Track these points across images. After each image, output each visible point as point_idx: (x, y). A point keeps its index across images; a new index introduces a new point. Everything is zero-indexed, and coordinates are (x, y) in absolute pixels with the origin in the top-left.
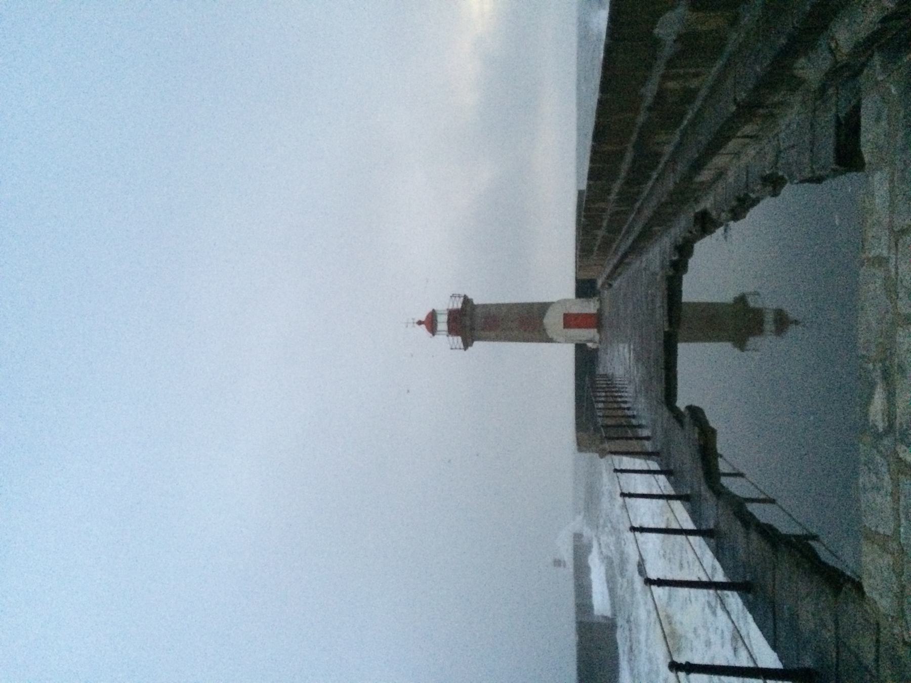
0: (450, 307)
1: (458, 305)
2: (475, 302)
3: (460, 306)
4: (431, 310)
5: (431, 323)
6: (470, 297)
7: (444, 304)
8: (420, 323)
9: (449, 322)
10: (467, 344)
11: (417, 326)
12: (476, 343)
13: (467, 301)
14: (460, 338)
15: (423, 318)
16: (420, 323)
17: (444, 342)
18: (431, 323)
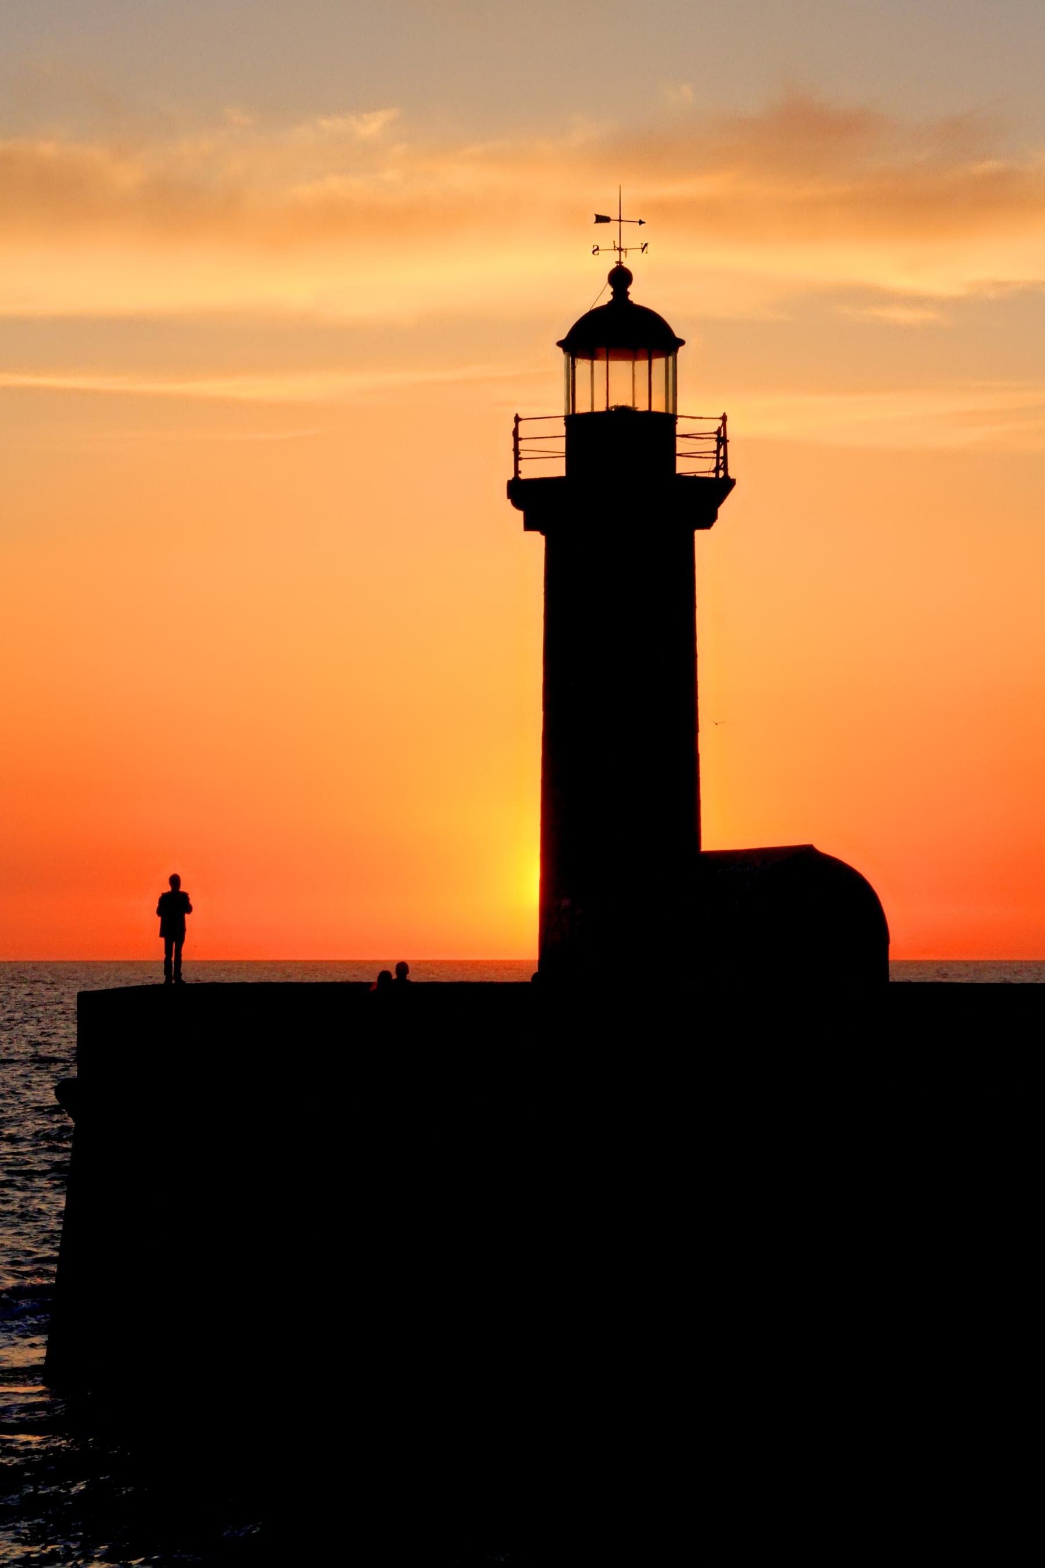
2: (699, 535)
3: (683, 466)
5: (621, 328)
8: (620, 278)
14: (549, 463)
15: (637, 295)
16: (620, 278)
17: (537, 403)
18: (621, 328)
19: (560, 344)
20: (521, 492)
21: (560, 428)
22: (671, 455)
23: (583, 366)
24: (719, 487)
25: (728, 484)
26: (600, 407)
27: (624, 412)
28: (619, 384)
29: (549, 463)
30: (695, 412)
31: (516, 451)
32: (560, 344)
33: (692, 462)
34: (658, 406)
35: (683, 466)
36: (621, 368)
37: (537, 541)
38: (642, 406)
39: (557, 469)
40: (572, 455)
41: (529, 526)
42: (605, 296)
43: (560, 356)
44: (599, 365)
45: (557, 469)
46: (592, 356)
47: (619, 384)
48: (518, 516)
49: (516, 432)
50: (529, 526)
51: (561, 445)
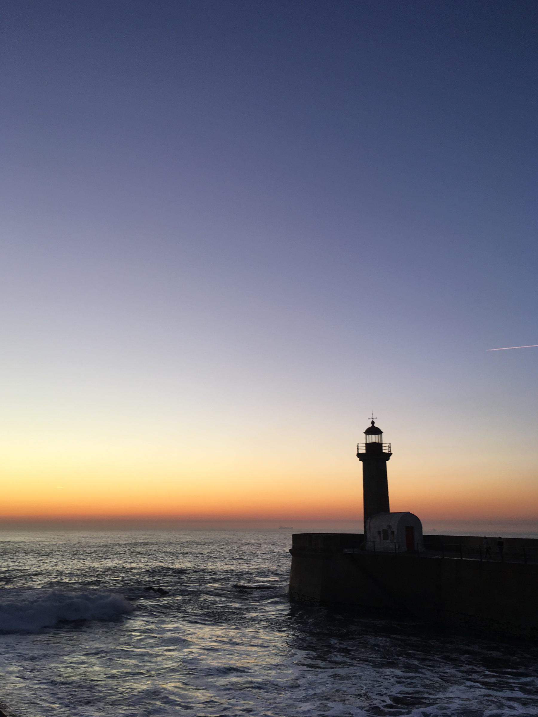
0: (383, 445)
1: (385, 450)
2: (387, 462)
3: (384, 451)
5: (373, 430)
6: (391, 457)
7: (387, 440)
8: (373, 423)
9: (374, 444)
10: (359, 455)
11: (371, 420)
13: (388, 456)
14: (363, 451)
15: (376, 425)
16: (373, 423)
18: (373, 430)
19: (364, 433)
21: (364, 445)
23: (368, 436)
24: (390, 454)
25: (391, 454)
26: (371, 442)
28: (373, 439)
31: (358, 449)
32: (364, 433)
35: (384, 451)
36: (373, 436)
37: (361, 463)
38: (377, 442)
39: (364, 451)
40: (367, 449)
41: (360, 460)
42: (371, 425)
43: (364, 435)
44: (370, 436)
46: (369, 434)
47: (373, 439)
48: (358, 459)
49: (358, 446)
50: (360, 460)
51: (365, 448)
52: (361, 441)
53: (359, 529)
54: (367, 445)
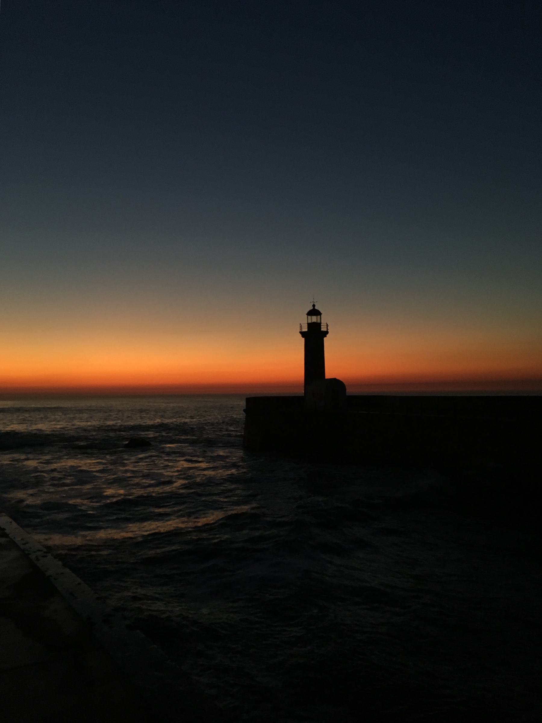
3: (322, 329)
4: (321, 312)
5: (314, 312)
7: (325, 320)
8: (314, 306)
9: (314, 323)
11: (312, 304)
12: (303, 340)
13: (327, 332)
14: (305, 329)
15: (316, 308)
16: (314, 306)
18: (314, 312)
20: (301, 333)
22: (320, 328)
27: (314, 323)
28: (314, 319)
29: (305, 329)
30: (324, 322)
33: (323, 329)
34: (319, 321)
35: (322, 329)
39: (306, 330)
42: (312, 308)
43: (306, 316)
45: (306, 330)
47: (314, 319)
52: (304, 321)
53: (301, 391)
54: (308, 324)
